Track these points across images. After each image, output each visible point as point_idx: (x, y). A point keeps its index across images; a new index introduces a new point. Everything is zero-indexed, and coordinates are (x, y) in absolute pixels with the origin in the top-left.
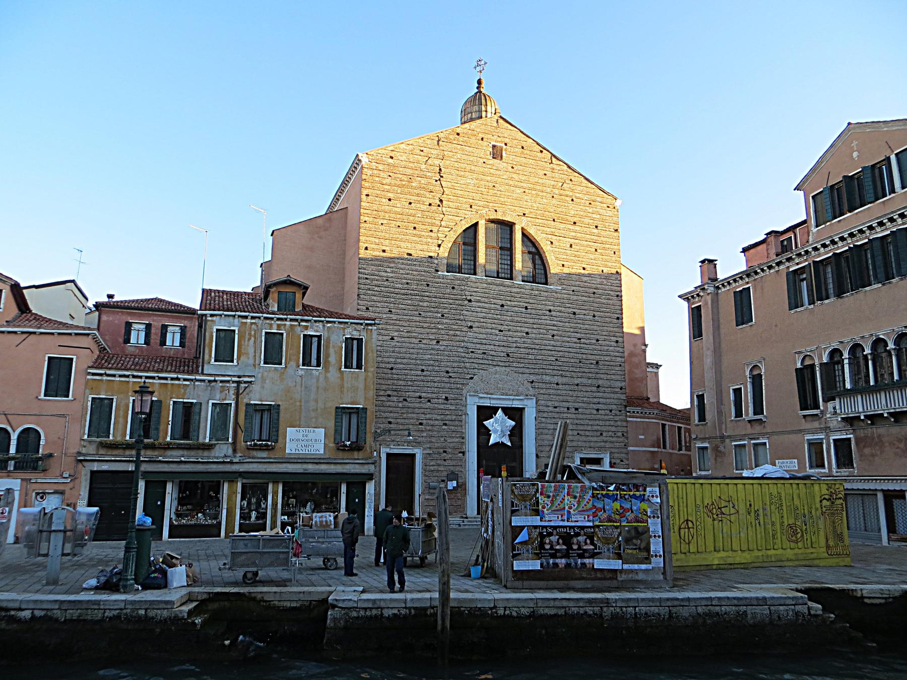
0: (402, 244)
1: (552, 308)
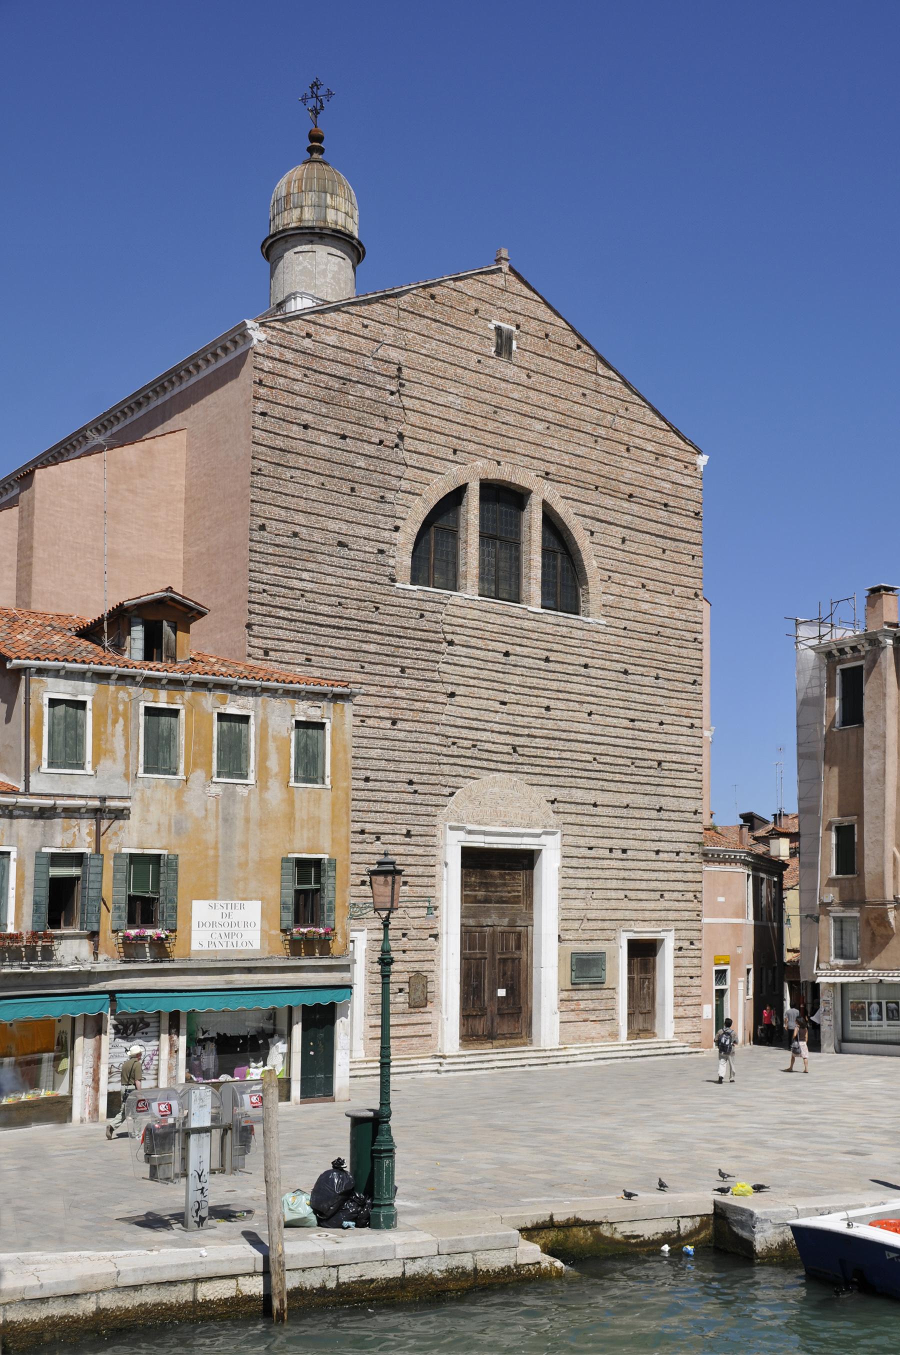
0: (332, 525)
1: (589, 661)
